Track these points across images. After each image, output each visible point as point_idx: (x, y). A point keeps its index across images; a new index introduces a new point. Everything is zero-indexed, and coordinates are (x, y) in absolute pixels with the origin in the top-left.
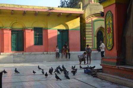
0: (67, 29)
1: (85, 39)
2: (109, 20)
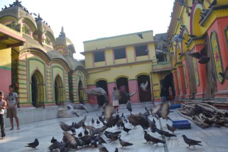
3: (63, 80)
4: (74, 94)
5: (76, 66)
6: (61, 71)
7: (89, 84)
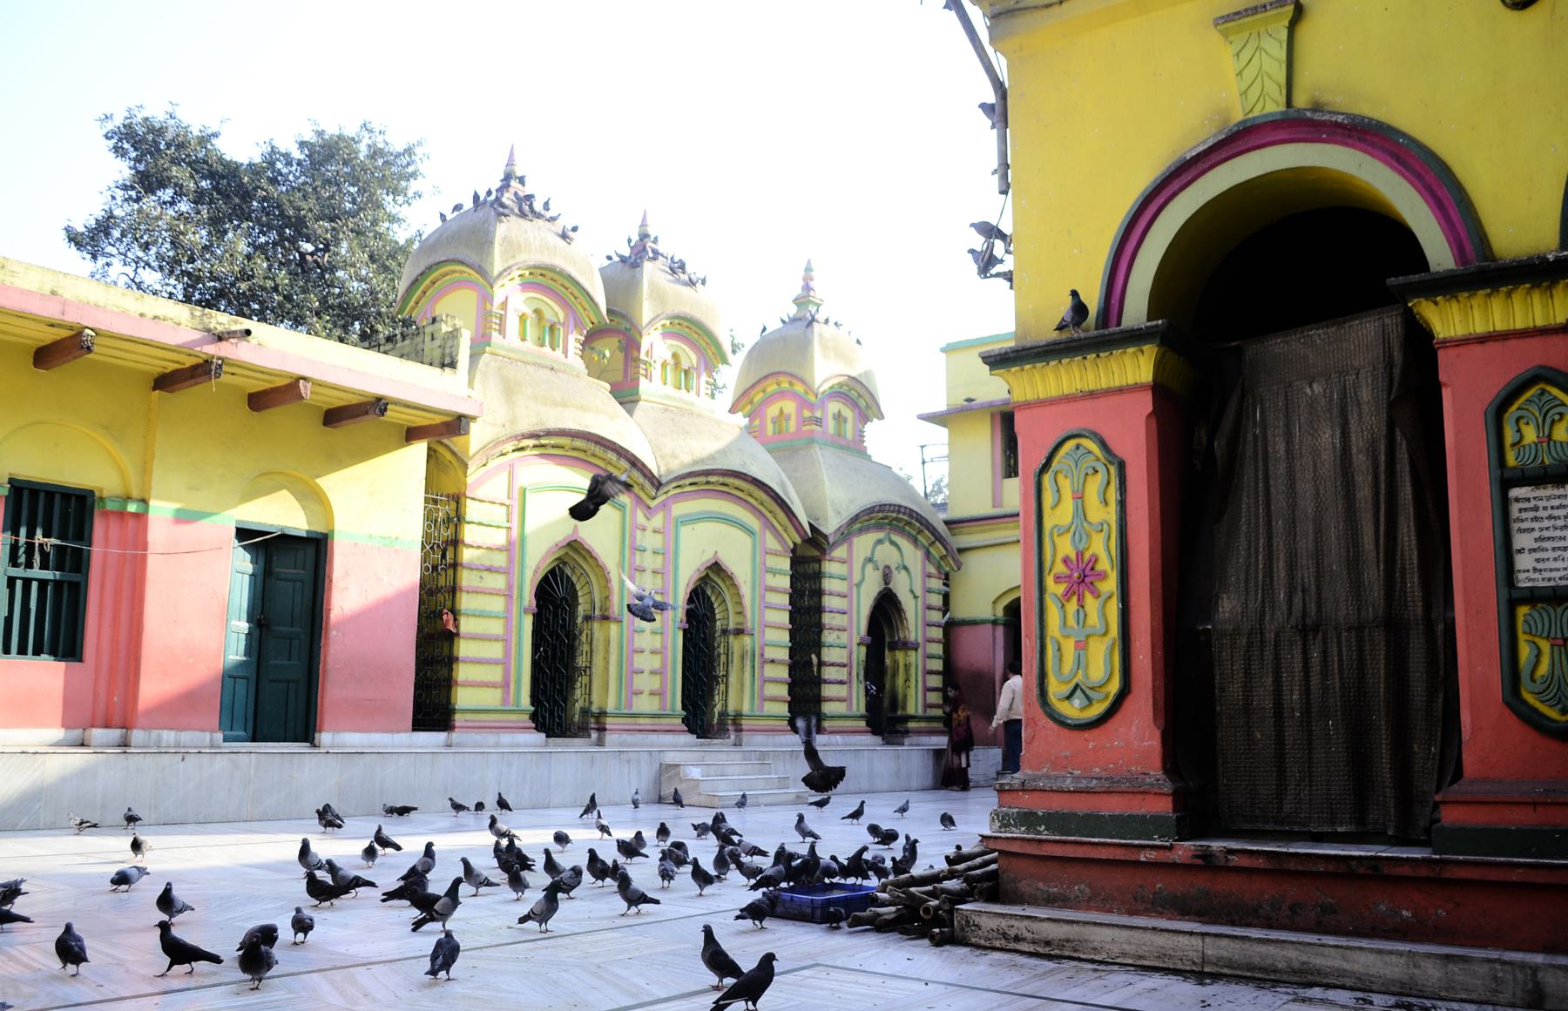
0: (319, 528)
1: (451, 627)
2: (1079, 497)
3: (746, 590)
4: (828, 673)
5: (854, 509)
6: (746, 540)
7: (961, 611)
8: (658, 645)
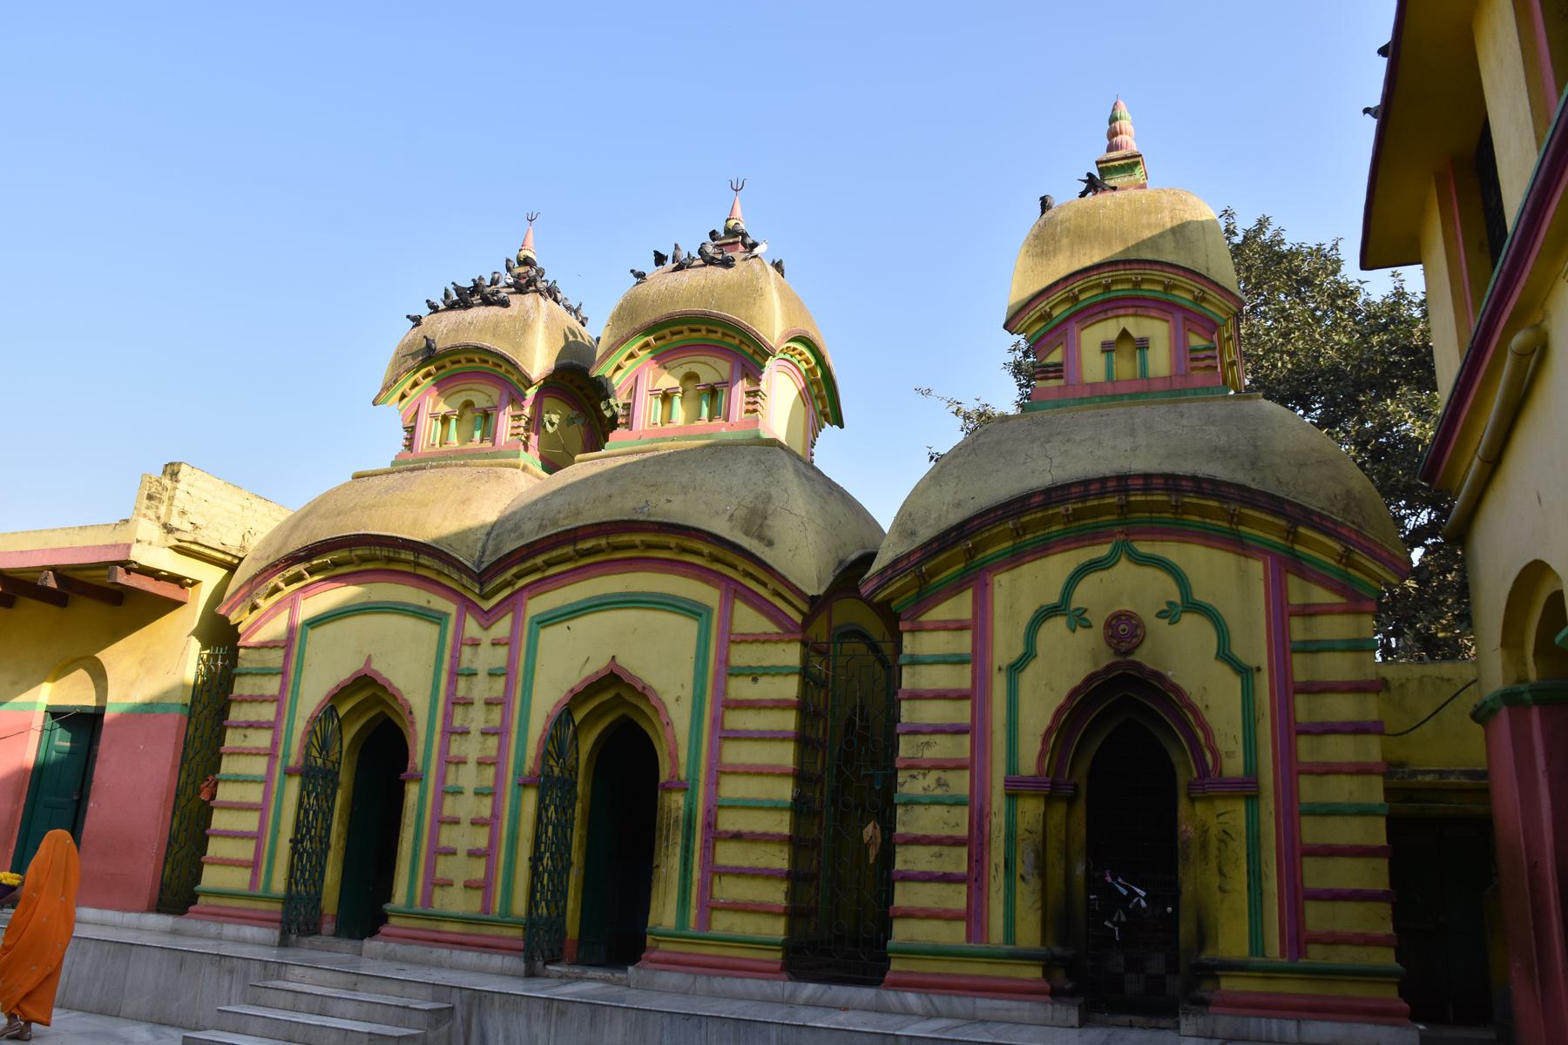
3: (679, 716)
6: (686, 628)
8: (486, 812)
